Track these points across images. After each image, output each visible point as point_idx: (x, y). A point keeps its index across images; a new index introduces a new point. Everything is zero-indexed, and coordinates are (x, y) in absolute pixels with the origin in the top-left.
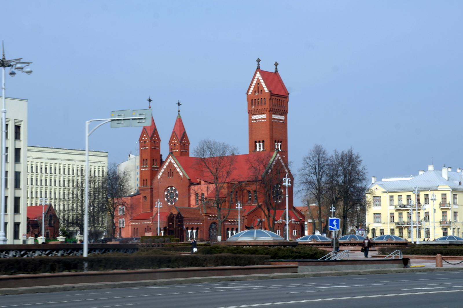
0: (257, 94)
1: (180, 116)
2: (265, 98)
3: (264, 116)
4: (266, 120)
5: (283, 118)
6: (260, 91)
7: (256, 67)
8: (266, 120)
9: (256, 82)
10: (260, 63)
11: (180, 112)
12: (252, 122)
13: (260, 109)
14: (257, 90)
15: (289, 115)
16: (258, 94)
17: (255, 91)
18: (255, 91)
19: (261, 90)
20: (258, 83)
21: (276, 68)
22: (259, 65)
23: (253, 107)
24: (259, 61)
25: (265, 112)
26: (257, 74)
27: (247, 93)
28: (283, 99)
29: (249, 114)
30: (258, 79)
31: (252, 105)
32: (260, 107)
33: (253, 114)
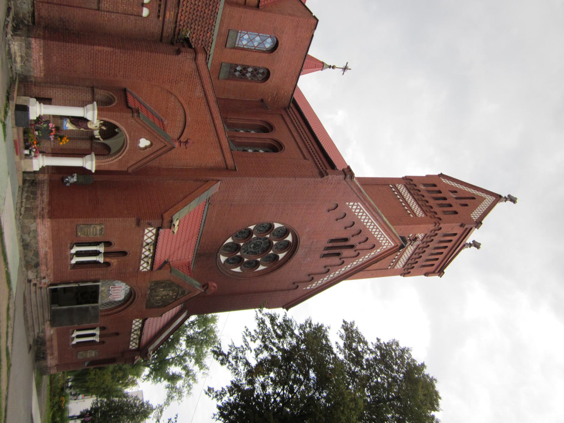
0: (454, 196)
1: (326, 68)
2: (456, 213)
3: (419, 213)
4: (411, 216)
5: (400, 265)
6: (463, 202)
7: (503, 195)
8: (411, 216)
9: (474, 194)
10: (508, 202)
11: (331, 68)
12: (391, 186)
13: (428, 202)
14: (460, 195)
15: (399, 278)
16: (457, 198)
17: (456, 192)
18: (456, 192)
19: (466, 205)
20: (474, 198)
21: (470, 245)
22: (506, 199)
23: (422, 187)
24: (513, 200)
25: (429, 214)
26: (490, 197)
27: (441, 175)
28: (436, 263)
29: (403, 178)
30: (483, 199)
31: (425, 185)
32: (432, 202)
33: (408, 186)
